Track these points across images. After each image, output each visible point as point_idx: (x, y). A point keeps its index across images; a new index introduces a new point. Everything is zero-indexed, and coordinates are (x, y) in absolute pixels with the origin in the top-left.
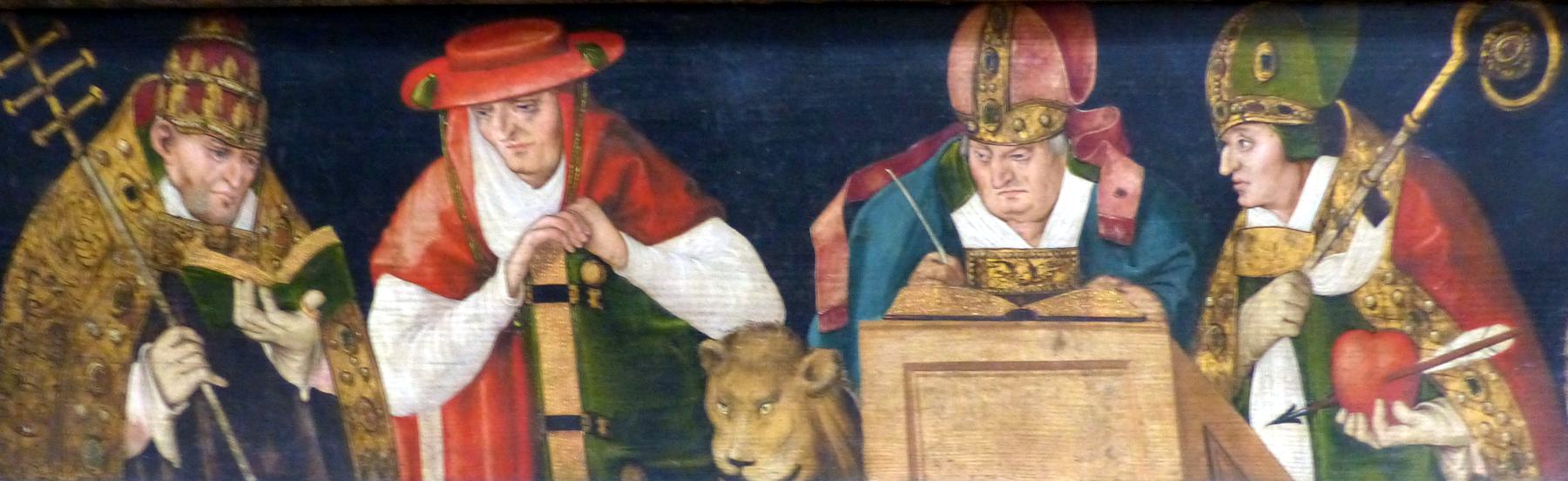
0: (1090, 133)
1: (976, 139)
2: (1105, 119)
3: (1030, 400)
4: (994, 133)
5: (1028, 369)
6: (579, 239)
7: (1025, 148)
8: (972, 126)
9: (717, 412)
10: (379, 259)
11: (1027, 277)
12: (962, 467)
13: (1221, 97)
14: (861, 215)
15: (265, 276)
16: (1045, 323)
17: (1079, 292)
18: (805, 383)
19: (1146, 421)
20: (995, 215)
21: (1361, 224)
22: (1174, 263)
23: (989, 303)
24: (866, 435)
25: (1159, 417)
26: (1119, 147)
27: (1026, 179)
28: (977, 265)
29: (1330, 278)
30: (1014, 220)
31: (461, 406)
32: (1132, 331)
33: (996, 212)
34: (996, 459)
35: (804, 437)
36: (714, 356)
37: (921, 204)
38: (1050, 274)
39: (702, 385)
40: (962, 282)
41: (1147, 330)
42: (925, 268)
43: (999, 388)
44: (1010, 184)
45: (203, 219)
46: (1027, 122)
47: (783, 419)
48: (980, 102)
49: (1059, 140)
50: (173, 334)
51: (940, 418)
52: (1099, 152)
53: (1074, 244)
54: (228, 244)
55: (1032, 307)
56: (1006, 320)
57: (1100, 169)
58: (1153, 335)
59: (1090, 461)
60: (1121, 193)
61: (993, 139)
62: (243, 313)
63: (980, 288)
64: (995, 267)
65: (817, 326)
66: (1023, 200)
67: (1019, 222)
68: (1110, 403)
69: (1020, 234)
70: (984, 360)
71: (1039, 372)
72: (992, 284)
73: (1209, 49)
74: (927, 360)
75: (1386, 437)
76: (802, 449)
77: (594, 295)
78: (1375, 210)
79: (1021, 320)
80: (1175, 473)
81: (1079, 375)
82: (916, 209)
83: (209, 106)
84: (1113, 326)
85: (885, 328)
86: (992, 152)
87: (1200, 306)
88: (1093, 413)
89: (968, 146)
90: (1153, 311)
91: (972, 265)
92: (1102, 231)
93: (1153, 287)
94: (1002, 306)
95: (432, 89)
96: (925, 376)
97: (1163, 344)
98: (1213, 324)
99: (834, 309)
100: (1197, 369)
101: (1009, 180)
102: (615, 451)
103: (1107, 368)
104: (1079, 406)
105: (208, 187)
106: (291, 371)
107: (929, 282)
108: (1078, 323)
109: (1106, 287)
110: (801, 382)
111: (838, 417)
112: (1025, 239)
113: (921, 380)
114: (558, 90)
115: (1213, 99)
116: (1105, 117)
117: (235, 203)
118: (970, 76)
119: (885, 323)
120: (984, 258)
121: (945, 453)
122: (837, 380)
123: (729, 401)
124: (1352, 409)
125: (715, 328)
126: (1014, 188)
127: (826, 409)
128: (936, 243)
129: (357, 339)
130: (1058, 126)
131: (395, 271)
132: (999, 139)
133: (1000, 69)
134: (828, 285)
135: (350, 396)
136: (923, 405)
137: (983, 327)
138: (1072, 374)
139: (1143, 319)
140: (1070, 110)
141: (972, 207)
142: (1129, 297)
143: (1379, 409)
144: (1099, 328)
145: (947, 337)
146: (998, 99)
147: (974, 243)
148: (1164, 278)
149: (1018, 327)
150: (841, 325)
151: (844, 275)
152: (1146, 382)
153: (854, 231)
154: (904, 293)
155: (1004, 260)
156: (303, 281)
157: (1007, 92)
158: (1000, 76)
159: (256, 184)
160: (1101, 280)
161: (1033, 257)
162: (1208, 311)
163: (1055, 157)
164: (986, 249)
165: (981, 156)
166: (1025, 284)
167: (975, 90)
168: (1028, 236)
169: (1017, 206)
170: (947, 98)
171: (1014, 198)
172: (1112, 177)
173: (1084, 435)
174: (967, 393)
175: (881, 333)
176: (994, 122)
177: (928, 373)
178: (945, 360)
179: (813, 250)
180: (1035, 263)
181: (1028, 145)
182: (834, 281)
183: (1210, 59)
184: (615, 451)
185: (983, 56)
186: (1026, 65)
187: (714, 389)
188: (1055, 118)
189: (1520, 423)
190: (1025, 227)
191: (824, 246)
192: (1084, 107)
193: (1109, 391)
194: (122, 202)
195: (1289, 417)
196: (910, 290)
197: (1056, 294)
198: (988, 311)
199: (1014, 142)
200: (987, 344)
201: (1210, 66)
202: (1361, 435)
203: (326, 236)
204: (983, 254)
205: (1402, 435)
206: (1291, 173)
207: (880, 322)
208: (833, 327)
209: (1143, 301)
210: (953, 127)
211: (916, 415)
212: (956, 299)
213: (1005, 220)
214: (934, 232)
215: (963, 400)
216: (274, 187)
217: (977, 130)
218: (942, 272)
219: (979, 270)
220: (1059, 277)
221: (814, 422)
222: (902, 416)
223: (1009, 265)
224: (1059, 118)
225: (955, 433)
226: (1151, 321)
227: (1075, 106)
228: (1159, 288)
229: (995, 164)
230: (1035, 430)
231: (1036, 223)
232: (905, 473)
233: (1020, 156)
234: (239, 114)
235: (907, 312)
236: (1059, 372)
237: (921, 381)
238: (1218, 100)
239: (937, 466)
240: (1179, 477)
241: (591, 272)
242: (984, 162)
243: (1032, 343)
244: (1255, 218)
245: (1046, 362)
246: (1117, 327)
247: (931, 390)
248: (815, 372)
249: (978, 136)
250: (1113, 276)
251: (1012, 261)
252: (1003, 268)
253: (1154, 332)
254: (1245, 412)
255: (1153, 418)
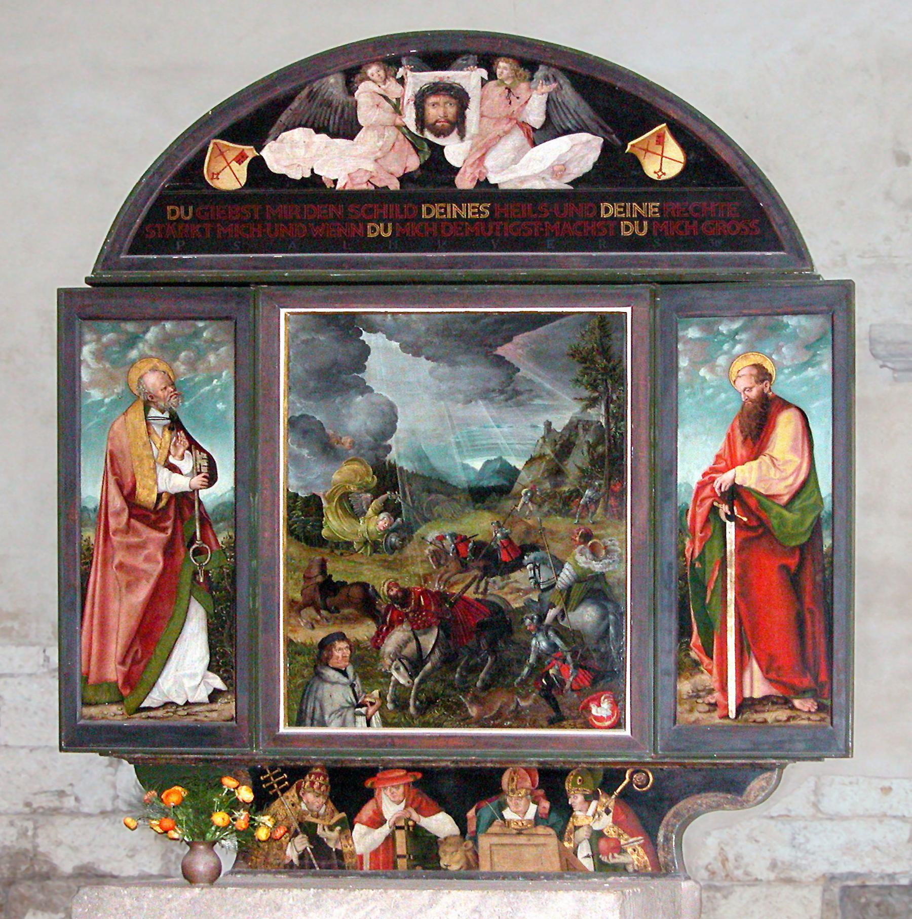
2: (541, 792)
6: (408, 816)
9: (441, 854)
10: (356, 820)
15: (327, 823)
21: (604, 814)
29: (597, 827)
31: (375, 854)
35: (464, 860)
36: (442, 842)
39: (438, 849)
42: (495, 823)
45: (312, 811)
47: (458, 856)
50: (300, 836)
54: (318, 816)
62: (319, 831)
65: (468, 836)
66: (520, 809)
75: (612, 861)
77: (411, 829)
78: (607, 812)
83: (315, 786)
94: (515, 832)
95: (372, 784)
101: (517, 805)
102: (415, 863)
105: (313, 803)
106: (331, 845)
110: (463, 848)
114: (405, 784)
117: (320, 807)
123: (445, 852)
124: (603, 855)
125: (442, 836)
127: (470, 854)
129: (349, 837)
131: (360, 822)
135: (345, 850)
143: (610, 855)
156: (336, 824)
159: (326, 803)
181: (522, 797)
184: (415, 863)
187: (441, 849)
189: (646, 858)
194: (290, 806)
195: (588, 856)
202: (606, 860)
203: (343, 814)
205: (616, 861)
206: (586, 804)
209: (551, 831)
216: (331, 804)
221: (466, 857)
224: (529, 792)
234: (323, 788)
237: (493, 848)
241: (411, 823)
243: (522, 840)
244: (577, 813)
254: (576, 855)
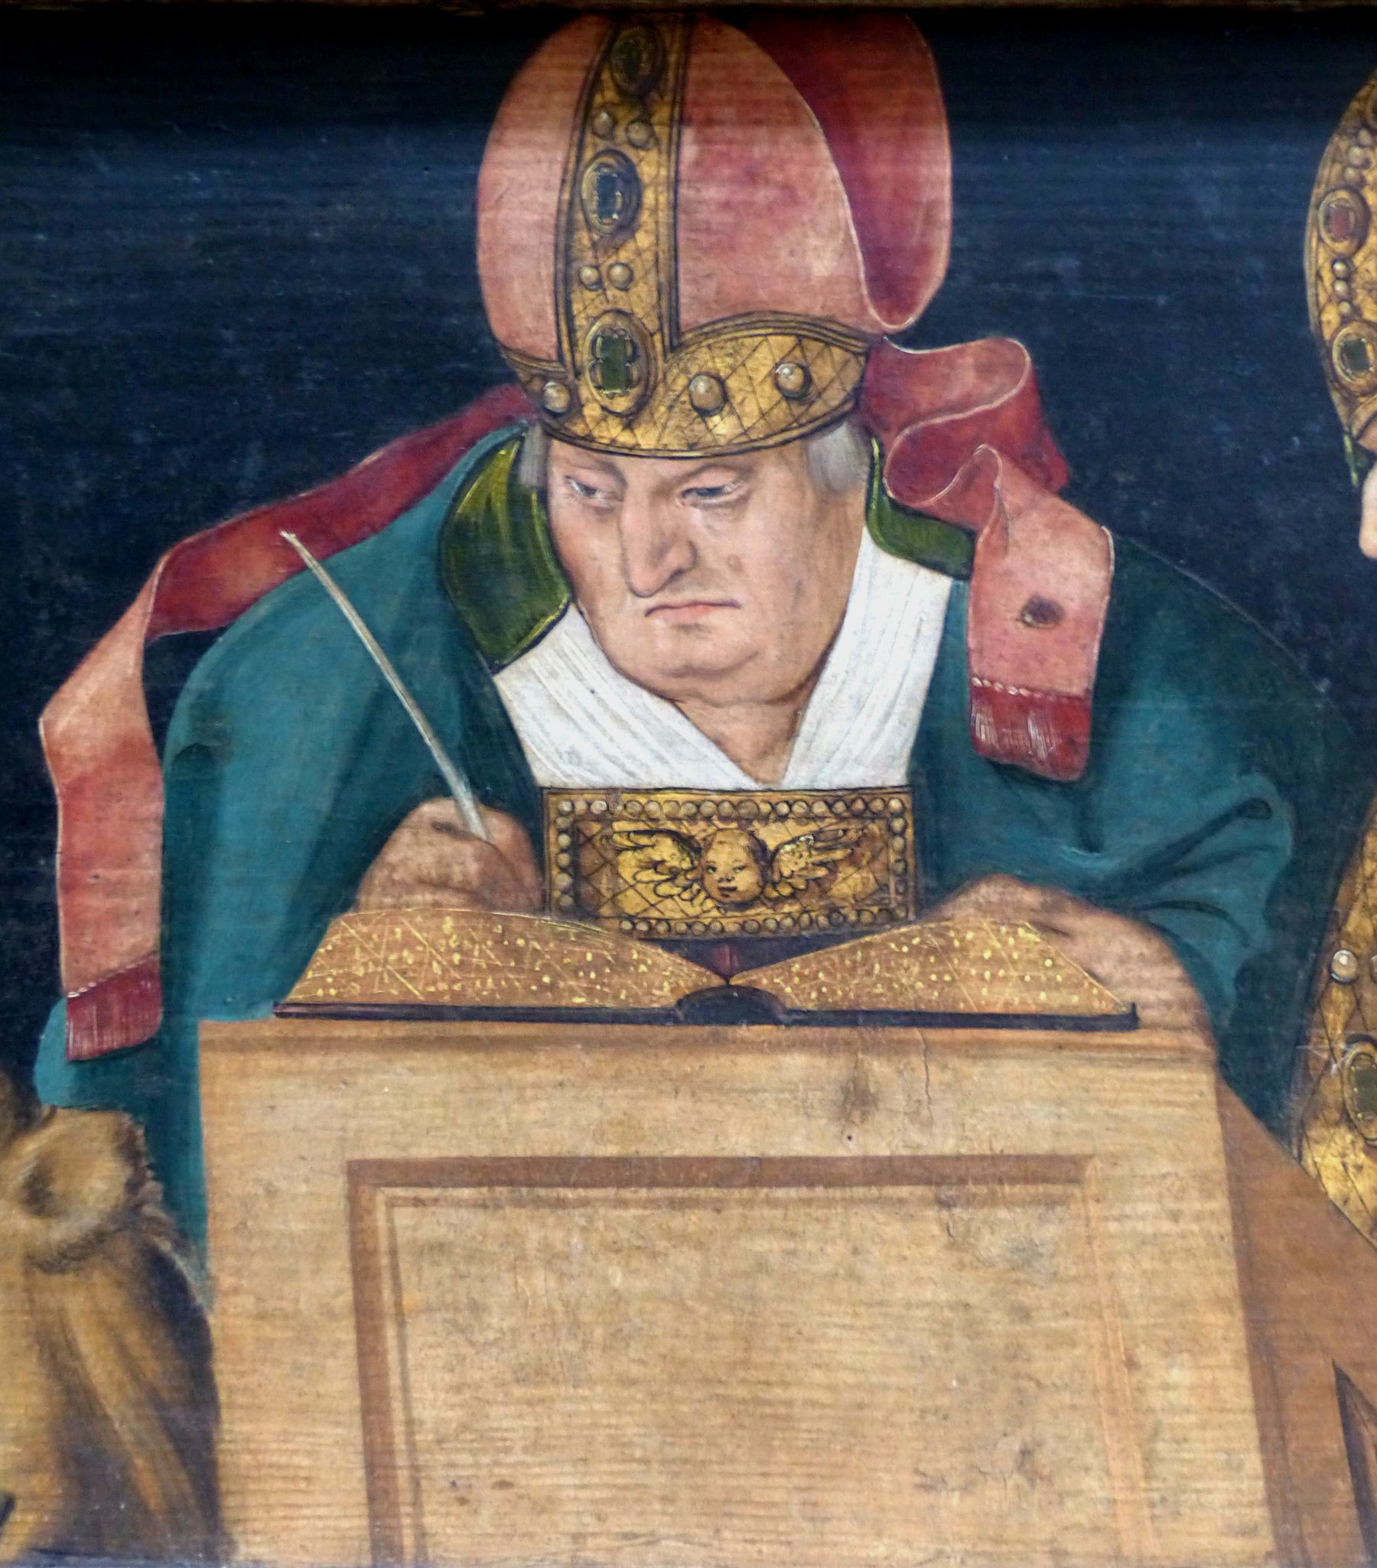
0: (938, 421)
1: (571, 440)
3: (765, 1286)
4: (629, 421)
5: (753, 1182)
7: (727, 467)
8: (556, 397)
11: (746, 881)
12: (544, 1505)
13: (1357, 310)
14: (198, 680)
16: (809, 1032)
17: (916, 933)
18: (23, 1223)
19: (1144, 1354)
20: (620, 671)
22: (1220, 842)
23: (621, 965)
24: (223, 1397)
25: (1195, 1345)
26: (1026, 463)
27: (737, 566)
28: (579, 841)
30: (697, 695)
32: (1091, 1061)
33: (646, 675)
34: (657, 1480)
37: (394, 644)
38: (821, 872)
40: (536, 896)
41: (1147, 1057)
43: (662, 1245)
44: (684, 580)
46: (732, 383)
48: (580, 321)
49: (839, 442)
51: (472, 1344)
52: (968, 483)
53: (897, 776)
55: (764, 979)
56: (677, 1022)
57: (972, 535)
58: (1158, 1075)
59: (966, 1489)
60: (1042, 612)
61: (625, 438)
63: (596, 918)
64: (638, 848)
67: (717, 705)
68: (1026, 1297)
69: (719, 743)
70: (612, 1150)
71: (793, 1193)
72: (631, 903)
73: (1313, 160)
74: (425, 1151)
76: (16, 1440)
79: (733, 1022)
80: (1248, 1531)
81: (924, 1201)
82: (380, 659)
84: (1037, 1046)
85: (286, 1045)
86: (623, 482)
87: (1312, 978)
88: (973, 1330)
89: (546, 458)
90: (1165, 995)
91: (565, 840)
92: (985, 734)
93: (1155, 916)
96: (418, 1202)
97: (1193, 1105)
98: (1351, 1041)
99: (122, 982)
100: (1310, 1186)
103: (1013, 1181)
104: (927, 1304)
107: (428, 897)
108: (916, 1034)
109: (1004, 916)
111: (133, 1337)
112: (736, 761)
113: (404, 1217)
115: (1331, 316)
116: (985, 370)
118: (550, 238)
119: (287, 1027)
120: (606, 818)
121: (485, 1460)
122: (129, 1214)
126: (688, 595)
128: (447, 769)
130: (835, 397)
132: (646, 437)
133: (645, 217)
134: (95, 903)
136: (411, 1297)
137: (604, 1043)
138: (901, 1201)
139: (1129, 1020)
140: (871, 349)
141: (562, 654)
142: (1079, 949)
144: (985, 1052)
145: (490, 1077)
146: (639, 312)
147: (568, 769)
148: (1190, 887)
149: (720, 1044)
150: (137, 1035)
151: (149, 869)
152: (1147, 1228)
153: (179, 732)
154: (343, 930)
155: (671, 826)
157: (669, 290)
158: (643, 239)
160: (987, 892)
161: (765, 819)
162: (1337, 994)
163: (829, 495)
164: (611, 791)
165: (589, 491)
166: (743, 905)
167: (565, 283)
168: (745, 749)
169: (703, 651)
170: (477, 307)
171: (697, 627)
172: (1012, 561)
173: (943, 1401)
174: (554, 1259)
175: (269, 1061)
176: (629, 383)
177: (425, 1193)
178: (480, 1150)
179: (48, 791)
180: (772, 835)
182: (115, 889)
183: (1318, 191)
185: (590, 175)
186: (726, 206)
188: (823, 371)
190: (736, 719)
191: (83, 779)
192: (909, 338)
193: (1025, 1256)
196: (366, 921)
197: (840, 940)
198: (623, 994)
199: (691, 447)
200: (618, 1101)
201: (1315, 215)
204: (599, 806)
207: (267, 1025)
208: (113, 1040)
210: (497, 398)
211: (390, 1332)
212: (516, 953)
213: (671, 700)
214: (439, 734)
215: (541, 1282)
217: (575, 406)
218: (466, 863)
219: (589, 858)
220: (849, 883)
222: (346, 1333)
223: (684, 842)
225: (518, 1392)
226: (1154, 1026)
227: (897, 337)
228: (1173, 920)
229: (634, 516)
230: (785, 1384)
231: (767, 709)
232: (356, 1523)
233: (713, 492)
235: (355, 992)
236: (860, 1192)
238: (1345, 320)
239: (463, 1501)
240: (1265, 1542)
242: (599, 511)
245: (816, 1160)
246: (1037, 1046)
247: (439, 1248)
248: (57, 1187)
249: (579, 429)
250: (1027, 881)
251: (698, 830)
252: (666, 850)
253: (1162, 1064)
255: (1169, 1350)
